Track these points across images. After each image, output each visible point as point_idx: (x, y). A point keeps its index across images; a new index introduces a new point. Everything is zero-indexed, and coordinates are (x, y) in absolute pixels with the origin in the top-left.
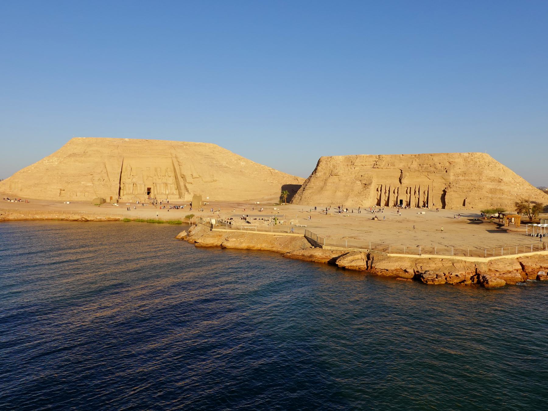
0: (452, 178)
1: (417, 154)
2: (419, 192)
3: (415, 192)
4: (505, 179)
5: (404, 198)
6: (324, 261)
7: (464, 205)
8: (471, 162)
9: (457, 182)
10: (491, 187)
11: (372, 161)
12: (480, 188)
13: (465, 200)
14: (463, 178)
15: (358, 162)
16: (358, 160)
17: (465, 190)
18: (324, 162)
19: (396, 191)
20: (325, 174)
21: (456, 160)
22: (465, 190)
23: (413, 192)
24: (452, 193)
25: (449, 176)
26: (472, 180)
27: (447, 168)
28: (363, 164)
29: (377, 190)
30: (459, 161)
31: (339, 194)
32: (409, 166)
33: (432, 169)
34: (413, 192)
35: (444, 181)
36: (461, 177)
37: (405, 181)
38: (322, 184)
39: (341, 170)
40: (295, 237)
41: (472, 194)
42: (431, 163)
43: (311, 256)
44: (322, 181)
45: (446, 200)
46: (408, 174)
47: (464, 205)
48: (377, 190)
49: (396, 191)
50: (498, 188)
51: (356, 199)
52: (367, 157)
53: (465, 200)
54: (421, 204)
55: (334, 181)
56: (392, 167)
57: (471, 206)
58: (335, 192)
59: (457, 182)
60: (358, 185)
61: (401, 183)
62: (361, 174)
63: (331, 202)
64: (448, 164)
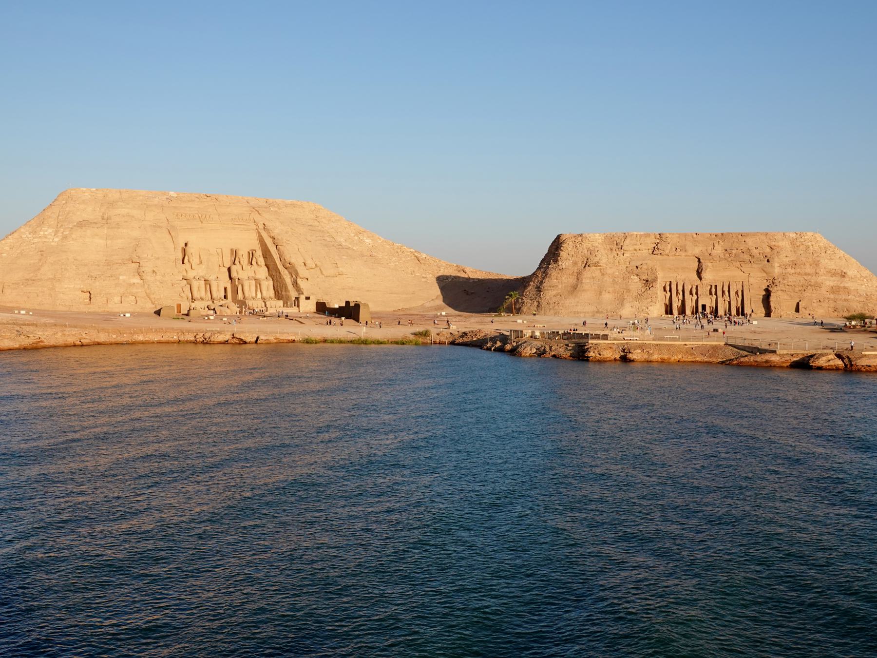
0: (777, 271)
1: (719, 232)
3: (723, 292)
4: (850, 273)
5: (706, 300)
6: (785, 365)
7: (797, 310)
8: (801, 247)
9: (784, 276)
10: (832, 284)
11: (650, 243)
12: (818, 286)
13: (798, 304)
14: (793, 271)
15: (628, 245)
16: (628, 241)
17: (797, 289)
18: (571, 243)
20: (575, 263)
21: (780, 244)
22: (797, 289)
23: (720, 293)
24: (780, 293)
25: (773, 267)
26: (806, 274)
27: (769, 256)
28: (637, 247)
29: (665, 290)
30: (784, 244)
31: (607, 297)
32: (710, 251)
33: (746, 257)
34: (720, 293)
35: (765, 275)
36: (790, 270)
38: (572, 280)
39: (603, 257)
40: (716, 346)
41: (807, 294)
42: (743, 247)
43: (767, 362)
44: (572, 274)
45: (772, 304)
46: (710, 264)
47: (797, 310)
48: (665, 290)
50: (842, 285)
51: (636, 304)
52: (641, 235)
53: (798, 304)
55: (594, 275)
56: (683, 254)
57: (808, 312)
58: (600, 293)
59: (784, 276)
60: (635, 283)
61: (700, 278)
62: (634, 264)
63: (595, 309)
64: (768, 250)
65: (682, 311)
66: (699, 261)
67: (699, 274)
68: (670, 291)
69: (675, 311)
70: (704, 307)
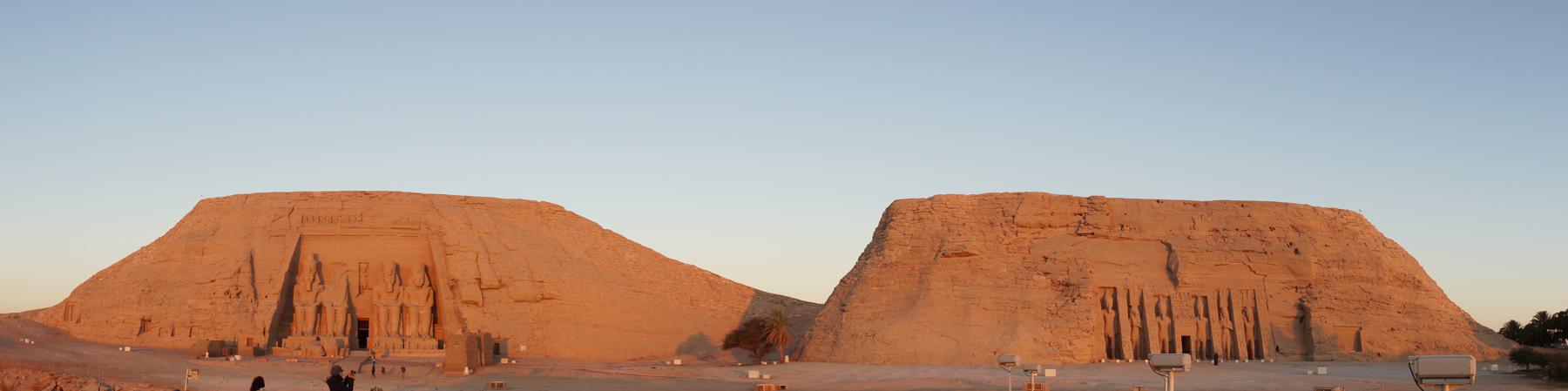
0: (1314, 271)
2: (1230, 309)
3: (1220, 310)
13: (1358, 334)
14: (1341, 272)
19: (1164, 308)
23: (1213, 313)
24: (1323, 313)
29: (1104, 306)
32: (1187, 232)
35: (1293, 278)
37: (1186, 274)
48: (1104, 306)
49: (1164, 308)
53: (1358, 334)
54: (1242, 350)
61: (1175, 281)
64: (1292, 235)
65: (1142, 352)
66: (1170, 250)
67: (1172, 273)
68: (1115, 307)
69: (1128, 350)
70: (1186, 340)
